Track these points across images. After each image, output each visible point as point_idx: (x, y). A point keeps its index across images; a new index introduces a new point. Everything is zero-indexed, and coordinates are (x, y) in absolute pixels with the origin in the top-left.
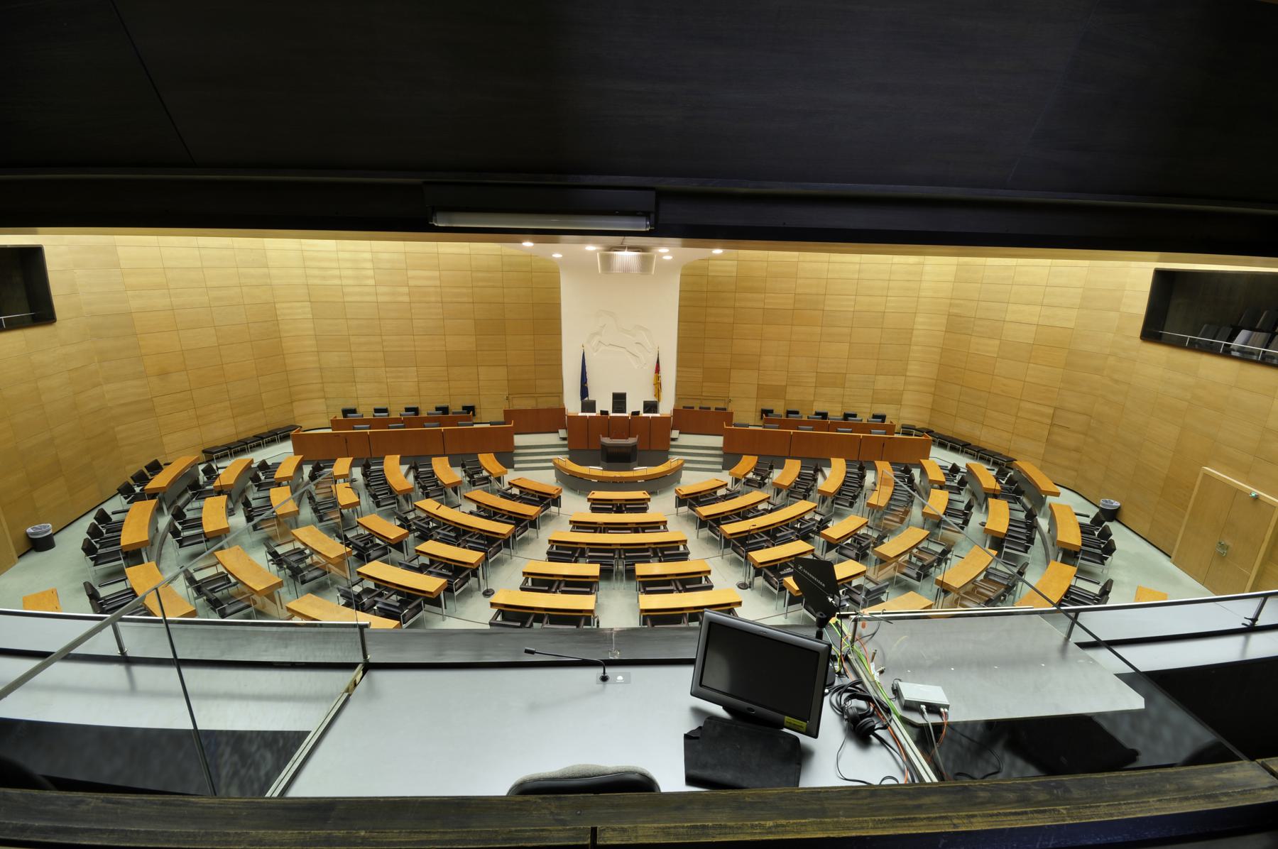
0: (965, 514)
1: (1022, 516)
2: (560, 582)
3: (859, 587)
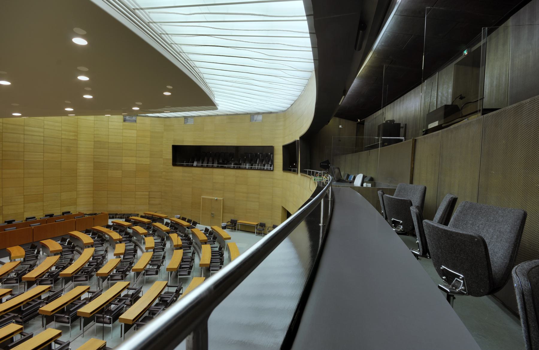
3: (126, 296)
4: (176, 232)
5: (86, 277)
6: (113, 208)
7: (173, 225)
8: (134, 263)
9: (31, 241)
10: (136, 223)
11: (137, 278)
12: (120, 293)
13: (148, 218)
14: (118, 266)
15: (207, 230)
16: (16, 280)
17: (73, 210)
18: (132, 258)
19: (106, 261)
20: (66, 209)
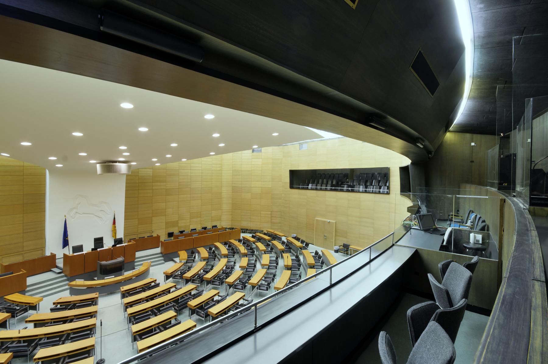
0: (276, 261)
1: (294, 258)
2: (65, 357)
4: (290, 252)
5: (219, 283)
6: (245, 224)
7: (288, 244)
8: (252, 277)
9: (192, 247)
10: (260, 239)
11: (252, 291)
12: (238, 302)
13: (269, 236)
14: (241, 277)
15: (317, 253)
16: (180, 277)
17: (220, 225)
18: (251, 271)
19: (234, 270)
20: (214, 224)
